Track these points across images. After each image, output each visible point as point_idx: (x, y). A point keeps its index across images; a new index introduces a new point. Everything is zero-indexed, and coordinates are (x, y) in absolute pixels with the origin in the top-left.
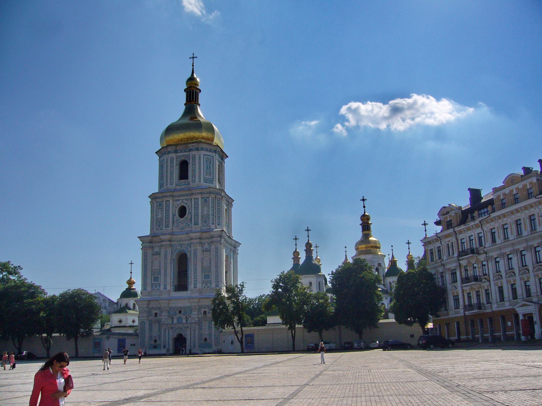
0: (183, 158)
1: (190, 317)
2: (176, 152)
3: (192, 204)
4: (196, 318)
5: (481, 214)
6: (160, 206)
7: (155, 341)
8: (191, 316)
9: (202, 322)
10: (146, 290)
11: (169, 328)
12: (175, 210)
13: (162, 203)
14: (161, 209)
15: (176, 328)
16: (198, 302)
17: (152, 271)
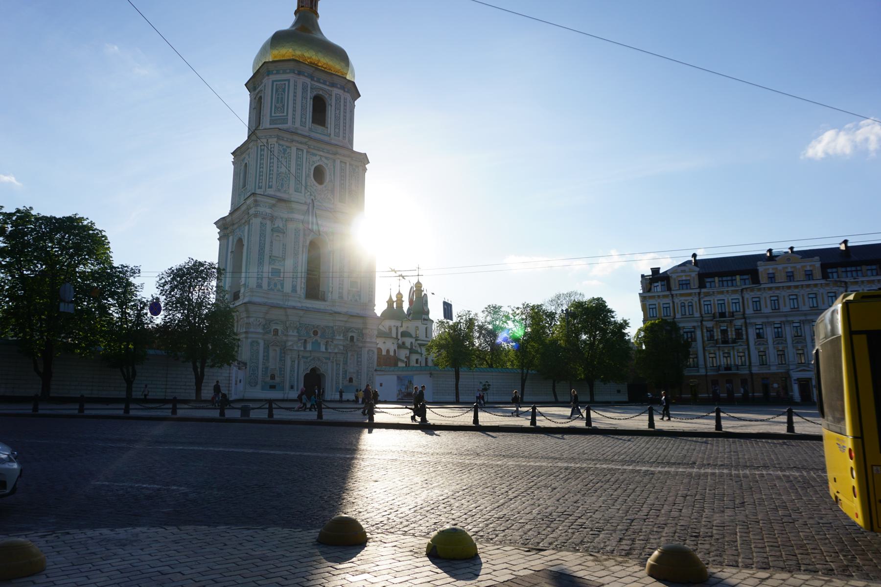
0: (321, 93)
1: (332, 342)
2: (312, 78)
3: (334, 167)
4: (341, 345)
5: (722, 281)
6: (284, 153)
7: (273, 377)
8: (334, 342)
9: (347, 353)
10: (261, 287)
11: (300, 357)
12: (310, 169)
13: (288, 150)
14: (286, 158)
15: (312, 357)
16: (346, 321)
17: (270, 256)
